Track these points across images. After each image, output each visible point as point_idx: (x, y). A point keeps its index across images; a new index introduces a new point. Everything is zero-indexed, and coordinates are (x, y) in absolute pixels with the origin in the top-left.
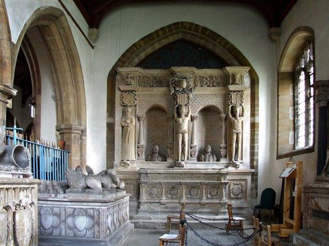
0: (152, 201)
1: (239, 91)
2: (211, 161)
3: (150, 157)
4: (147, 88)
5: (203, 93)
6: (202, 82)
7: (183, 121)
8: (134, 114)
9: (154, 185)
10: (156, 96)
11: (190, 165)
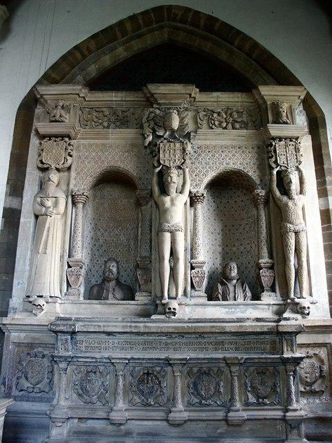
0: (86, 414)
2: (240, 300)
5: (214, 143)
6: (211, 118)
8: (64, 188)
9: (92, 369)
10: (110, 149)
11: (191, 309)
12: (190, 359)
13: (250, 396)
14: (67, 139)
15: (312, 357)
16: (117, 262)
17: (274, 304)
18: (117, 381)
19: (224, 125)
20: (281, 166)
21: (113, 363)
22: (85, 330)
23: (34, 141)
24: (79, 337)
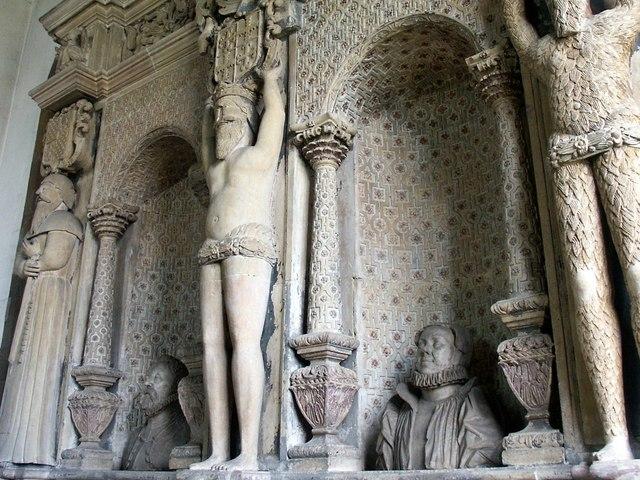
7: (227, 181)
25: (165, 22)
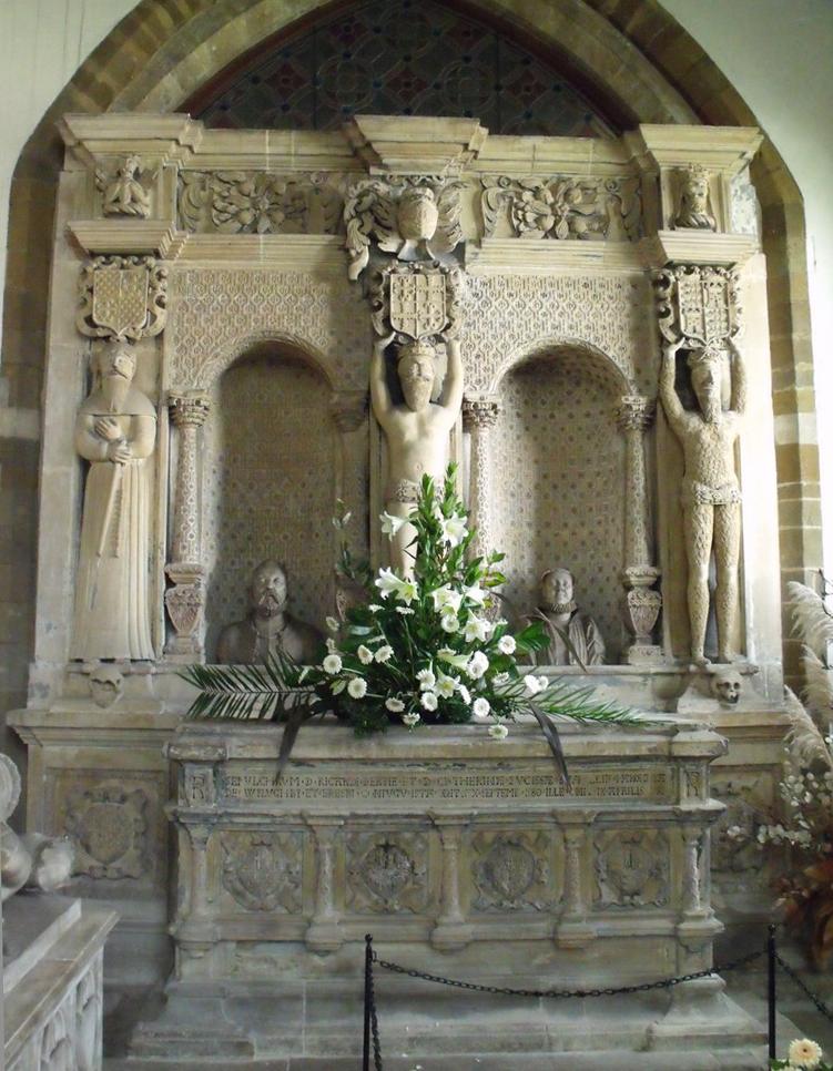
1: (715, 268)
3: (233, 636)
4: (227, 239)
6: (517, 208)
8: (150, 385)
9: (264, 836)
12: (480, 815)
13: (604, 888)
14: (152, 261)
15: (737, 795)
16: (284, 569)
17: (656, 674)
18: (319, 864)
19: (549, 223)
20: (687, 339)
21: (310, 826)
22: (247, 755)
23: (64, 265)
24: (231, 771)
25: (253, 195)
